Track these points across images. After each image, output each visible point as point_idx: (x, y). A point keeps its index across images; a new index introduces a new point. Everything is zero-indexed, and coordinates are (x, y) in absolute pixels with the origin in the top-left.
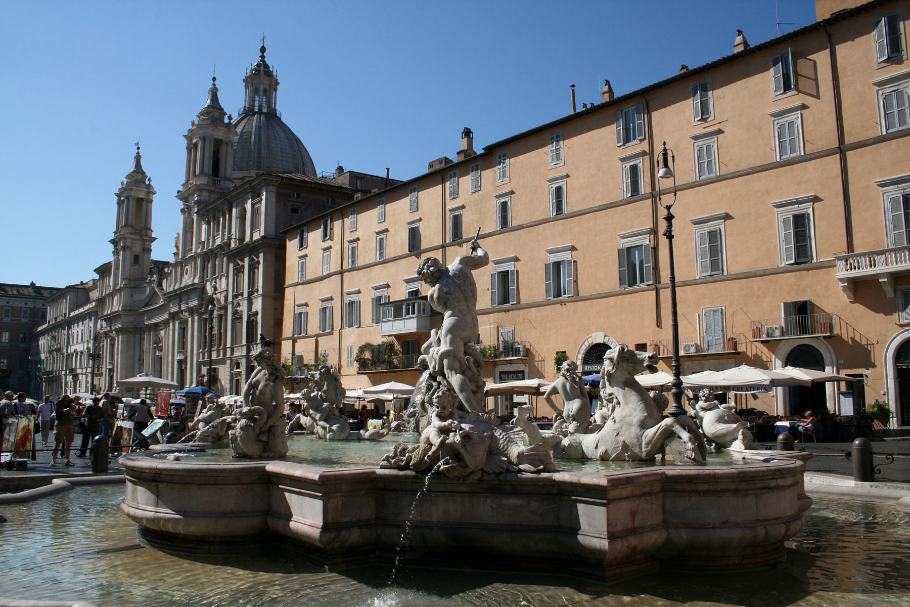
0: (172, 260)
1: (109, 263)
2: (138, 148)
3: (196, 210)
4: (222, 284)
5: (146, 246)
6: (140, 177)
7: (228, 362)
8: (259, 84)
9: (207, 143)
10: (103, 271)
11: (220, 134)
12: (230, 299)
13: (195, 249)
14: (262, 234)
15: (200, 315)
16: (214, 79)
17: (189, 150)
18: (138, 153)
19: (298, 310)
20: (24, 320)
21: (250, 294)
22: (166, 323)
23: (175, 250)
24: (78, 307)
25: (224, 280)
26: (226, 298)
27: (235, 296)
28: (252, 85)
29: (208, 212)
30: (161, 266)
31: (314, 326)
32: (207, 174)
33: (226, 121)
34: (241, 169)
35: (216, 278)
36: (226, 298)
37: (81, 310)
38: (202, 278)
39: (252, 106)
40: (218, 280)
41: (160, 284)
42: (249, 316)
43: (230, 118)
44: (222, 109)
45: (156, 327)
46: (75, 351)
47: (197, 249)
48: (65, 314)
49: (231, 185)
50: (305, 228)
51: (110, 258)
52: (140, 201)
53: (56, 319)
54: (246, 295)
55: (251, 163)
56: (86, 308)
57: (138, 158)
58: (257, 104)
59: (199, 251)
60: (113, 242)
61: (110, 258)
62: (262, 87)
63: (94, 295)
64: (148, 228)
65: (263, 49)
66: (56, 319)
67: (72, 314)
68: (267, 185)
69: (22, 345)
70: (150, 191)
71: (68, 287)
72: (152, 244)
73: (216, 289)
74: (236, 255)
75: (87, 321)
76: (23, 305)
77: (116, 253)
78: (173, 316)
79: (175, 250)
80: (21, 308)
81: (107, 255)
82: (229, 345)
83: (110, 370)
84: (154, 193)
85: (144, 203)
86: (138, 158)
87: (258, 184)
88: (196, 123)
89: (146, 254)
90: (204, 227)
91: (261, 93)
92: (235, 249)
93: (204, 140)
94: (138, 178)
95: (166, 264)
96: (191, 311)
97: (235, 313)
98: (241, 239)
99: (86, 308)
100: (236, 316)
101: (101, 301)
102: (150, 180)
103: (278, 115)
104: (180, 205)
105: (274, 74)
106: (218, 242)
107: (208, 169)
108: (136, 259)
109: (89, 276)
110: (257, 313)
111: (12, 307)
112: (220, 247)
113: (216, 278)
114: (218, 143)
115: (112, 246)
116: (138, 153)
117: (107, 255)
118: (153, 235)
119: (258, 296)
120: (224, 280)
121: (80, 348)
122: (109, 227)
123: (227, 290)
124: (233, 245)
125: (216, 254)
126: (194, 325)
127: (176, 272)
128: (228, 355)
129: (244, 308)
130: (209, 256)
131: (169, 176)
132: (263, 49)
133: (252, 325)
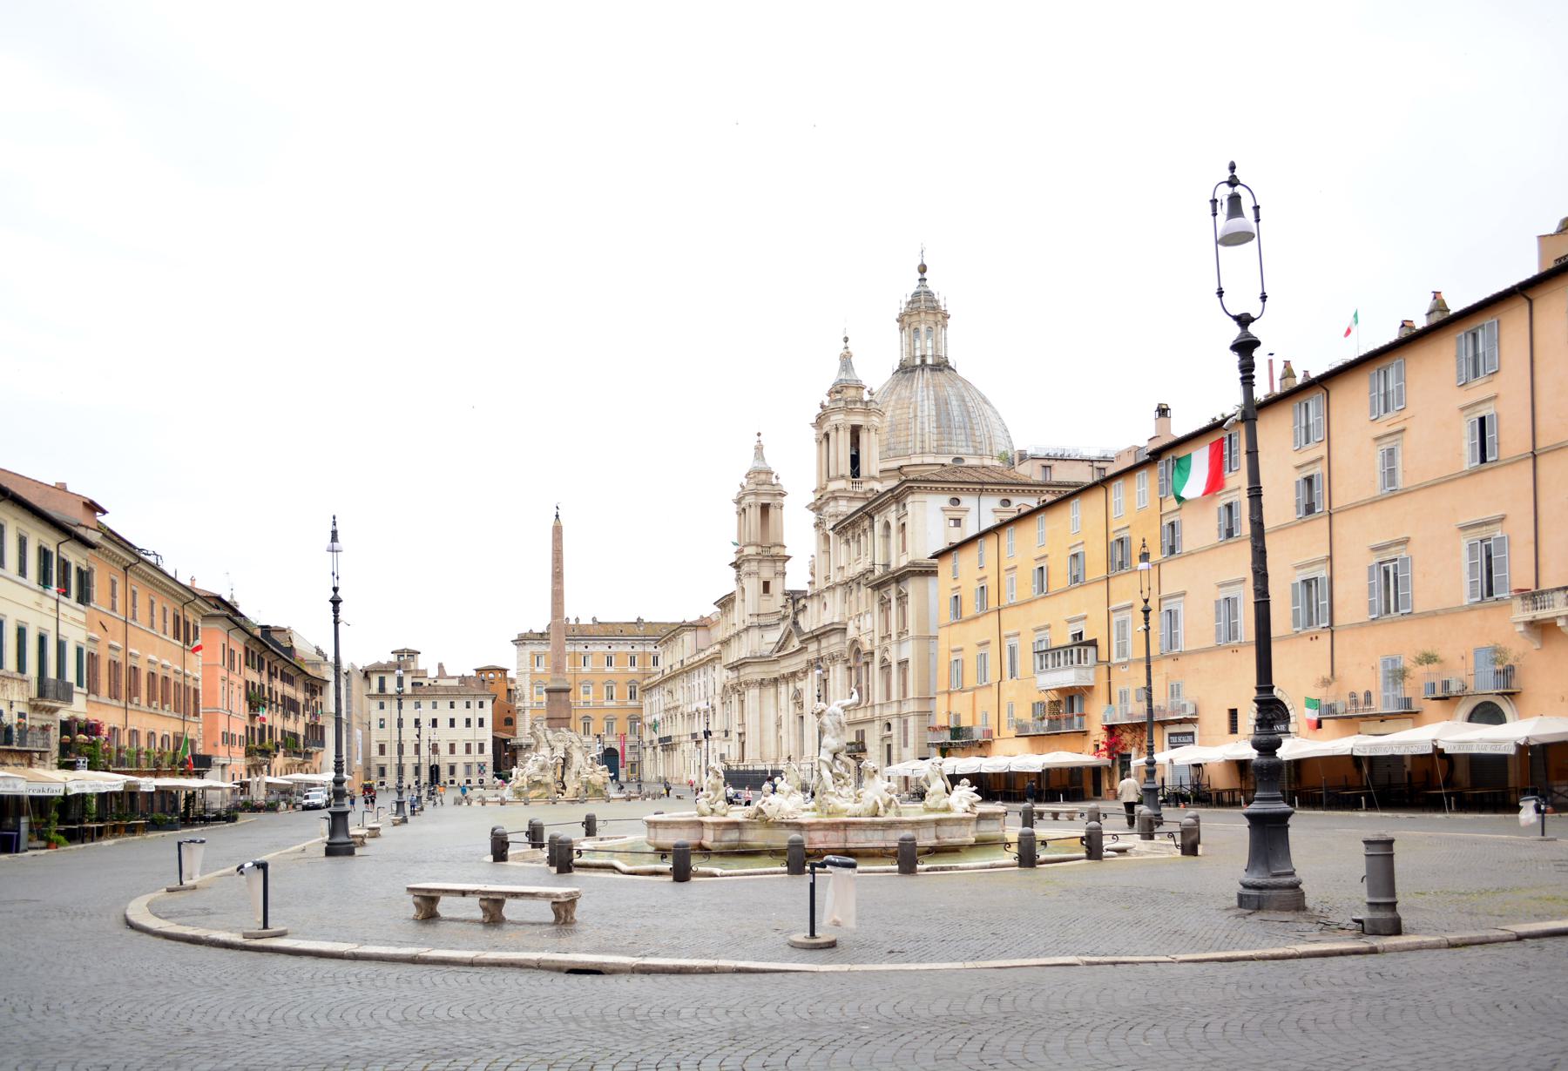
9: (841, 432)
10: (726, 603)
12: (877, 643)
21: (900, 634)
23: (810, 578)
24: (699, 651)
30: (794, 597)
32: (843, 477)
37: (702, 655)
41: (795, 623)
45: (794, 674)
54: (894, 637)
63: (719, 634)
69: (631, 703)
74: (879, 586)
75: (710, 669)
77: (738, 579)
78: (815, 664)
79: (810, 578)
81: (728, 584)
84: (782, 495)
85: (772, 511)
86: (759, 450)
89: (779, 580)
90: (844, 547)
95: (803, 594)
96: (833, 659)
97: (884, 660)
98: (887, 565)
101: (725, 643)
104: (812, 517)
107: (846, 468)
108: (766, 585)
109: (710, 610)
115: (733, 571)
126: (838, 674)
129: (893, 658)
130: (849, 585)
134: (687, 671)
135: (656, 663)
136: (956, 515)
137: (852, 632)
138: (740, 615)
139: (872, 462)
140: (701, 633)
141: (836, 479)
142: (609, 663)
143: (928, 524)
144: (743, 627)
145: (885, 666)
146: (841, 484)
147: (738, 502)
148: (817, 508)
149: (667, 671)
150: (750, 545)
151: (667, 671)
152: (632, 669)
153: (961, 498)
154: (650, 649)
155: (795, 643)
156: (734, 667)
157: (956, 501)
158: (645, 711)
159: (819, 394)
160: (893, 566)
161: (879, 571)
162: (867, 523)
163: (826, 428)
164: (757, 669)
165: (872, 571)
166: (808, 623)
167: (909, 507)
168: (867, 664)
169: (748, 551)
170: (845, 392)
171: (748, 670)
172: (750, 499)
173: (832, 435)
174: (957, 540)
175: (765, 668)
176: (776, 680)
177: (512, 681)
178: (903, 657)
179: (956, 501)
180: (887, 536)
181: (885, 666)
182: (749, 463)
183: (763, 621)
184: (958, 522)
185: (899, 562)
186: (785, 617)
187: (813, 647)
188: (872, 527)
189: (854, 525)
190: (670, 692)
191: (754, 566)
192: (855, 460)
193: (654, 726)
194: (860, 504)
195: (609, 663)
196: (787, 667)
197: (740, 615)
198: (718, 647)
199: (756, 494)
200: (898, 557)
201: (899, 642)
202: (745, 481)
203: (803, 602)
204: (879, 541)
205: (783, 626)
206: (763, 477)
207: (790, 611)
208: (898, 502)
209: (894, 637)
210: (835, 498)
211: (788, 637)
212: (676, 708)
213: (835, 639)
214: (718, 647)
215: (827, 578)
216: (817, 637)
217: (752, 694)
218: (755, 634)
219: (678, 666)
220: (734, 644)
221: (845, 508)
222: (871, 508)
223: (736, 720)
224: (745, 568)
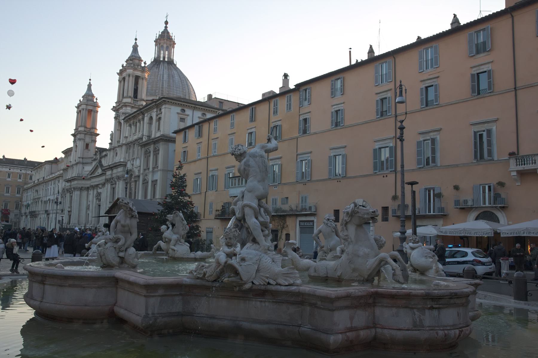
1: (71, 148)
2: (90, 80)
3: (123, 118)
4: (137, 163)
5: (93, 139)
8: (164, 43)
9: (131, 78)
10: (67, 152)
11: (138, 73)
12: (142, 172)
13: (123, 141)
14: (162, 133)
15: (125, 180)
16: (136, 39)
17: (120, 81)
18: (90, 83)
20: (19, 180)
21: (153, 168)
22: (104, 185)
23: (110, 141)
24: (52, 174)
25: (138, 161)
26: (139, 171)
27: (145, 170)
28: (160, 44)
29: (129, 119)
30: (102, 150)
32: (130, 97)
33: (143, 65)
34: (151, 95)
35: (134, 159)
36: (139, 171)
37: (53, 175)
38: (125, 158)
39: (159, 56)
40: (135, 160)
41: (100, 162)
42: (152, 182)
43: (145, 63)
44: (140, 58)
45: (97, 186)
46: (49, 200)
47: (123, 141)
48: (44, 178)
49: (144, 103)
50: (187, 130)
51: (71, 145)
52: (90, 111)
53: (38, 180)
54: (151, 169)
55: (157, 91)
56: (56, 174)
57: (90, 86)
58: (162, 56)
59: (124, 142)
60: (73, 135)
61: (71, 145)
62: (165, 46)
65: (166, 23)
66: (38, 180)
67: (48, 178)
68: (165, 104)
69: (18, 195)
71: (46, 162)
72: (98, 138)
73: (133, 165)
74: (145, 145)
76: (19, 171)
79: (110, 141)
80: (18, 173)
81: (69, 143)
83: (69, 211)
84: (99, 107)
85: (92, 113)
86: (90, 86)
88: (125, 65)
89: (93, 144)
90: (128, 128)
91: (165, 49)
92: (146, 141)
93: (129, 76)
95: (104, 150)
96: (119, 178)
97: (144, 180)
99: (56, 174)
100: (145, 181)
101: (65, 170)
102: (96, 99)
103: (175, 63)
104: (113, 114)
105: (173, 38)
107: (131, 94)
110: (156, 181)
111: (12, 173)
112: (136, 140)
113: (134, 159)
114: (137, 78)
115: (72, 138)
116: (90, 83)
117: (69, 143)
118: (98, 132)
119: (158, 171)
120: (138, 161)
121: (52, 198)
122: (72, 128)
123: (140, 166)
124: (144, 140)
125: (134, 144)
127: (110, 155)
129: (150, 178)
130: (129, 145)
131: (107, 97)
132: (166, 23)
134: (45, 182)
135: (31, 179)
137: (129, 166)
139: (143, 94)
140: (54, 166)
141: (128, 97)
142: (9, 177)
143: (170, 119)
144: (74, 163)
145: (145, 182)
146: (129, 100)
147: (78, 107)
148: (115, 109)
149: (36, 182)
150: (81, 126)
151: (36, 182)
152: (19, 180)
153: (186, 109)
154: (29, 172)
155: (100, 171)
156: (68, 181)
157: (183, 111)
158: (24, 199)
159: (122, 61)
160: (153, 136)
161: (144, 140)
162: (141, 117)
164: (80, 182)
165: (142, 139)
166: (105, 162)
167: (163, 110)
168: (136, 181)
169: (80, 129)
170: (134, 59)
171: (76, 182)
172: (84, 106)
173: (127, 78)
174: (181, 128)
175: (84, 182)
176: (88, 188)
178: (155, 179)
179: (183, 111)
180: (150, 123)
181: (145, 182)
182: (84, 91)
183: (85, 161)
184: (182, 120)
185: (155, 134)
186: (95, 160)
187: (109, 173)
188: (143, 119)
189: (134, 117)
190: (37, 191)
191: (82, 136)
192: (136, 91)
193: (28, 206)
194: (135, 110)
195: (9, 177)
196: (95, 182)
197: (73, 159)
198: (61, 172)
199: (87, 105)
200: (156, 132)
201: (153, 172)
202: (82, 99)
203: (104, 153)
204: (146, 126)
205: (94, 163)
206: (90, 98)
207: (98, 157)
208: (157, 108)
209: (151, 169)
210: (126, 106)
211: (96, 169)
212: (39, 198)
213: (120, 169)
214: (61, 172)
215: (119, 142)
216: (111, 168)
217: (76, 193)
218: (80, 166)
219: (42, 179)
221: (129, 110)
222: (142, 111)
223: (68, 205)
224: (78, 137)
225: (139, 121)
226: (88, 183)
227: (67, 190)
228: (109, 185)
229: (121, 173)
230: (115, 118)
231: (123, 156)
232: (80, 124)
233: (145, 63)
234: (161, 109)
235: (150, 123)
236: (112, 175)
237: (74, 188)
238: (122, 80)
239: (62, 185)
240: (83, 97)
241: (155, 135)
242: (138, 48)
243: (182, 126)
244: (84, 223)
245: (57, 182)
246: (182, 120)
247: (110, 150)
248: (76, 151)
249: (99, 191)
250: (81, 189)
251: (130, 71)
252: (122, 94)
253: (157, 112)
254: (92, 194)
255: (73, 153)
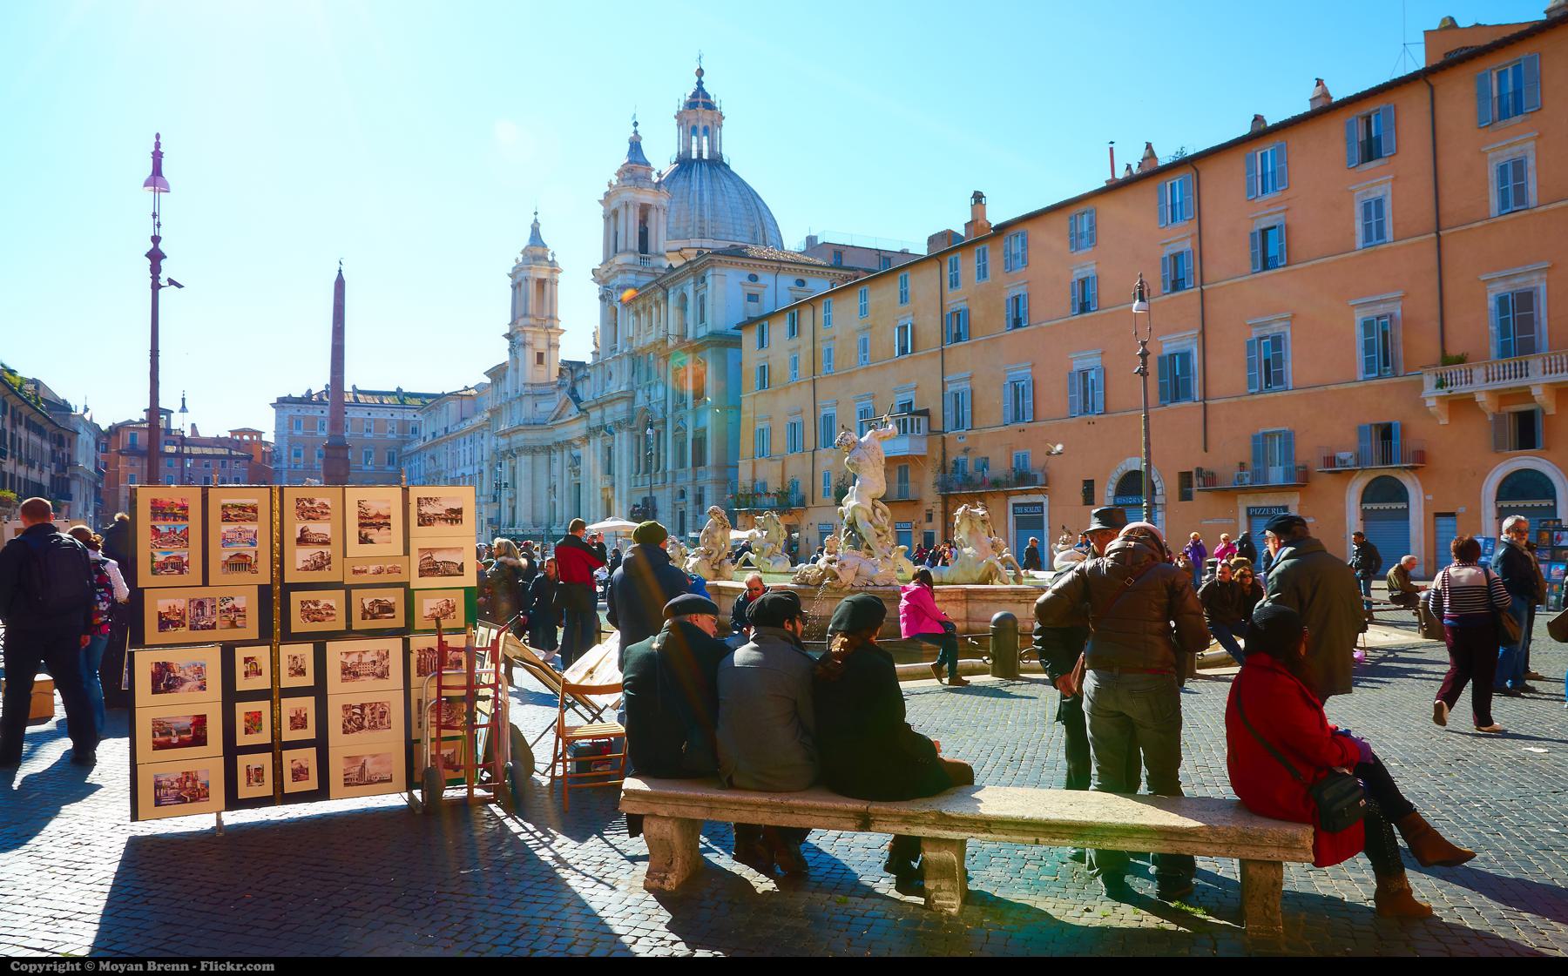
0: (589, 360)
6: (539, 251)
7: (669, 490)
9: (631, 210)
10: (497, 373)
12: (670, 410)
16: (636, 124)
17: (607, 218)
19: (760, 426)
22: (586, 439)
24: (463, 419)
26: (665, 409)
27: (676, 408)
30: (573, 369)
31: (780, 442)
32: (633, 252)
33: (655, 179)
43: (659, 174)
44: (647, 164)
52: (541, 283)
54: (690, 406)
60: (509, 336)
64: (552, 317)
70: (554, 268)
72: (562, 340)
78: (592, 432)
82: (669, 468)
85: (547, 286)
87: (702, 266)
89: (553, 352)
90: (632, 318)
94: (536, 250)
95: (582, 365)
96: (619, 425)
101: (495, 412)
106: (651, 338)
107: (634, 243)
108: (540, 357)
110: (705, 430)
114: (644, 210)
121: (468, 471)
122: (502, 319)
124: (671, 343)
126: (623, 443)
128: (669, 479)
131: (580, 250)
133: (699, 443)
136: (754, 290)
137: (641, 400)
138: (508, 386)
139: (660, 240)
141: (626, 251)
146: (630, 258)
153: (759, 274)
157: (753, 278)
163: (615, 204)
165: (665, 341)
167: (709, 280)
171: (521, 436)
173: (622, 212)
176: (549, 447)
177: (267, 443)
178: (701, 425)
179: (753, 278)
180: (683, 307)
181: (680, 430)
186: (560, 387)
188: (666, 298)
190: (433, 458)
200: (696, 328)
203: (581, 373)
204: (673, 313)
207: (568, 380)
209: (690, 406)
214: (487, 415)
216: (601, 405)
218: (528, 404)
220: (506, 416)
225: (657, 304)
226: (548, 437)
227: (504, 454)
228: (599, 440)
229: (624, 416)
230: (602, 298)
231: (626, 377)
232: (519, 312)
233: (659, 174)
234: (703, 279)
235: (683, 307)
236: (602, 418)
237: (520, 450)
238: (611, 216)
239: (489, 444)
240: (523, 252)
241: (695, 333)
242: (642, 143)
243: (754, 310)
244: (545, 521)
245: (478, 436)
246: (752, 298)
247: (594, 366)
248: (517, 370)
249: (575, 452)
250: (533, 451)
251: (628, 195)
252: (613, 245)
253: (696, 283)
254: (560, 460)
255: (510, 372)
